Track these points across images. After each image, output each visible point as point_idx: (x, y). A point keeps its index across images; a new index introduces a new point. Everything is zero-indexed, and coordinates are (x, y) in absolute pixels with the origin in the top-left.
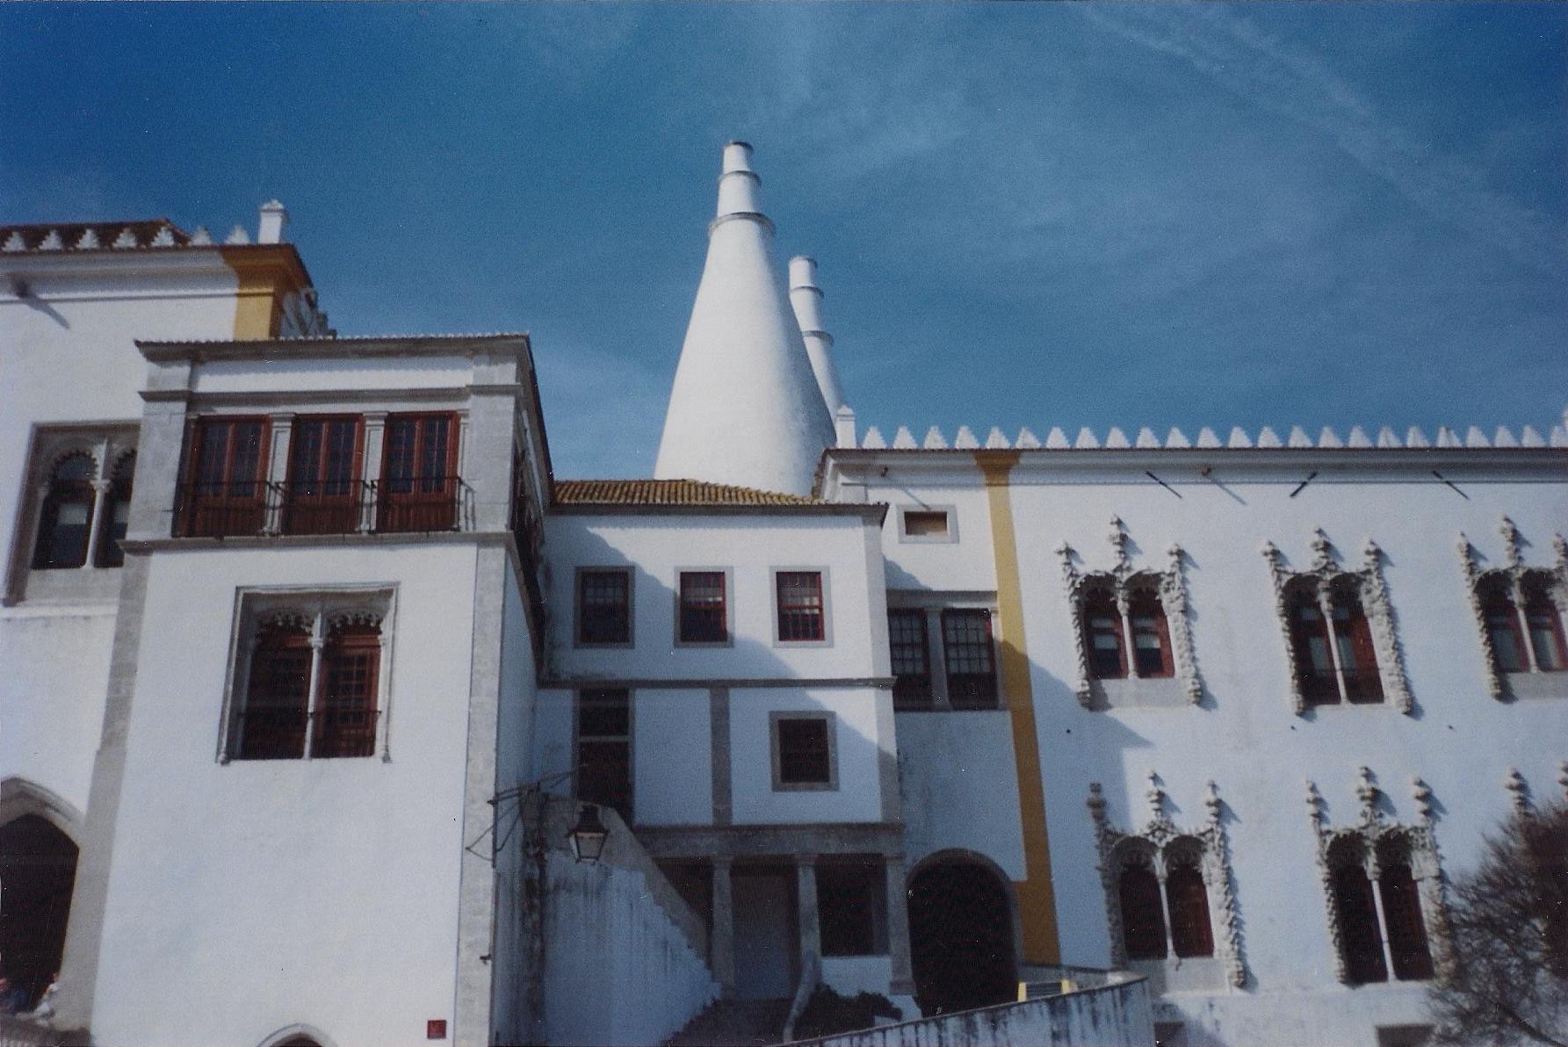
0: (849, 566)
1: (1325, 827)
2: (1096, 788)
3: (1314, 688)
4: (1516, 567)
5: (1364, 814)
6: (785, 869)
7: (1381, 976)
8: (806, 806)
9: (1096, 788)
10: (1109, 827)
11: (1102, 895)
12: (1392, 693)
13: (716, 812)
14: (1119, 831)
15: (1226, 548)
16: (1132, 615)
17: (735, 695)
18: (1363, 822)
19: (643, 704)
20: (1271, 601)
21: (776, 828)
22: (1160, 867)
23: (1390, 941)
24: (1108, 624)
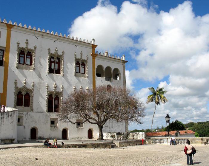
1: (48, 90)
2: (16, 80)
3: (51, 71)
4: (81, 59)
9: (16, 80)
11: (14, 96)
12: (62, 73)
14: (18, 87)
16: (27, 55)
22: (24, 93)
24: (23, 56)
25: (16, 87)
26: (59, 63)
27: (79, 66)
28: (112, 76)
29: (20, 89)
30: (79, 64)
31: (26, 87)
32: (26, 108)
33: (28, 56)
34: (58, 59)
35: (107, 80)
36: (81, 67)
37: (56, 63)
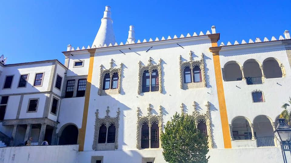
0: (48, 71)
3: (144, 89)
4: (191, 61)
5: (148, 114)
6: (25, 126)
7: (148, 147)
8: (32, 115)
9: (97, 110)
10: (98, 118)
13: (17, 117)
15: (131, 63)
17: (25, 96)
18: (148, 115)
19: (11, 99)
20: (138, 72)
21: (25, 119)
22: (108, 125)
23: (151, 140)
25: (98, 119)
26: (156, 77)
27: (189, 72)
28: (263, 74)
29: (103, 120)
30: (190, 70)
31: (110, 117)
32: (110, 144)
33: (114, 79)
34: (155, 71)
35: (249, 82)
36: (194, 73)
37: (153, 77)
